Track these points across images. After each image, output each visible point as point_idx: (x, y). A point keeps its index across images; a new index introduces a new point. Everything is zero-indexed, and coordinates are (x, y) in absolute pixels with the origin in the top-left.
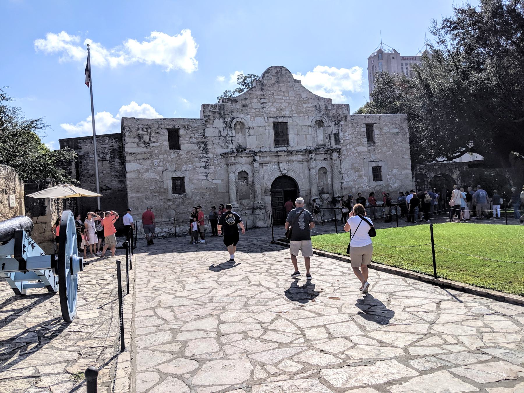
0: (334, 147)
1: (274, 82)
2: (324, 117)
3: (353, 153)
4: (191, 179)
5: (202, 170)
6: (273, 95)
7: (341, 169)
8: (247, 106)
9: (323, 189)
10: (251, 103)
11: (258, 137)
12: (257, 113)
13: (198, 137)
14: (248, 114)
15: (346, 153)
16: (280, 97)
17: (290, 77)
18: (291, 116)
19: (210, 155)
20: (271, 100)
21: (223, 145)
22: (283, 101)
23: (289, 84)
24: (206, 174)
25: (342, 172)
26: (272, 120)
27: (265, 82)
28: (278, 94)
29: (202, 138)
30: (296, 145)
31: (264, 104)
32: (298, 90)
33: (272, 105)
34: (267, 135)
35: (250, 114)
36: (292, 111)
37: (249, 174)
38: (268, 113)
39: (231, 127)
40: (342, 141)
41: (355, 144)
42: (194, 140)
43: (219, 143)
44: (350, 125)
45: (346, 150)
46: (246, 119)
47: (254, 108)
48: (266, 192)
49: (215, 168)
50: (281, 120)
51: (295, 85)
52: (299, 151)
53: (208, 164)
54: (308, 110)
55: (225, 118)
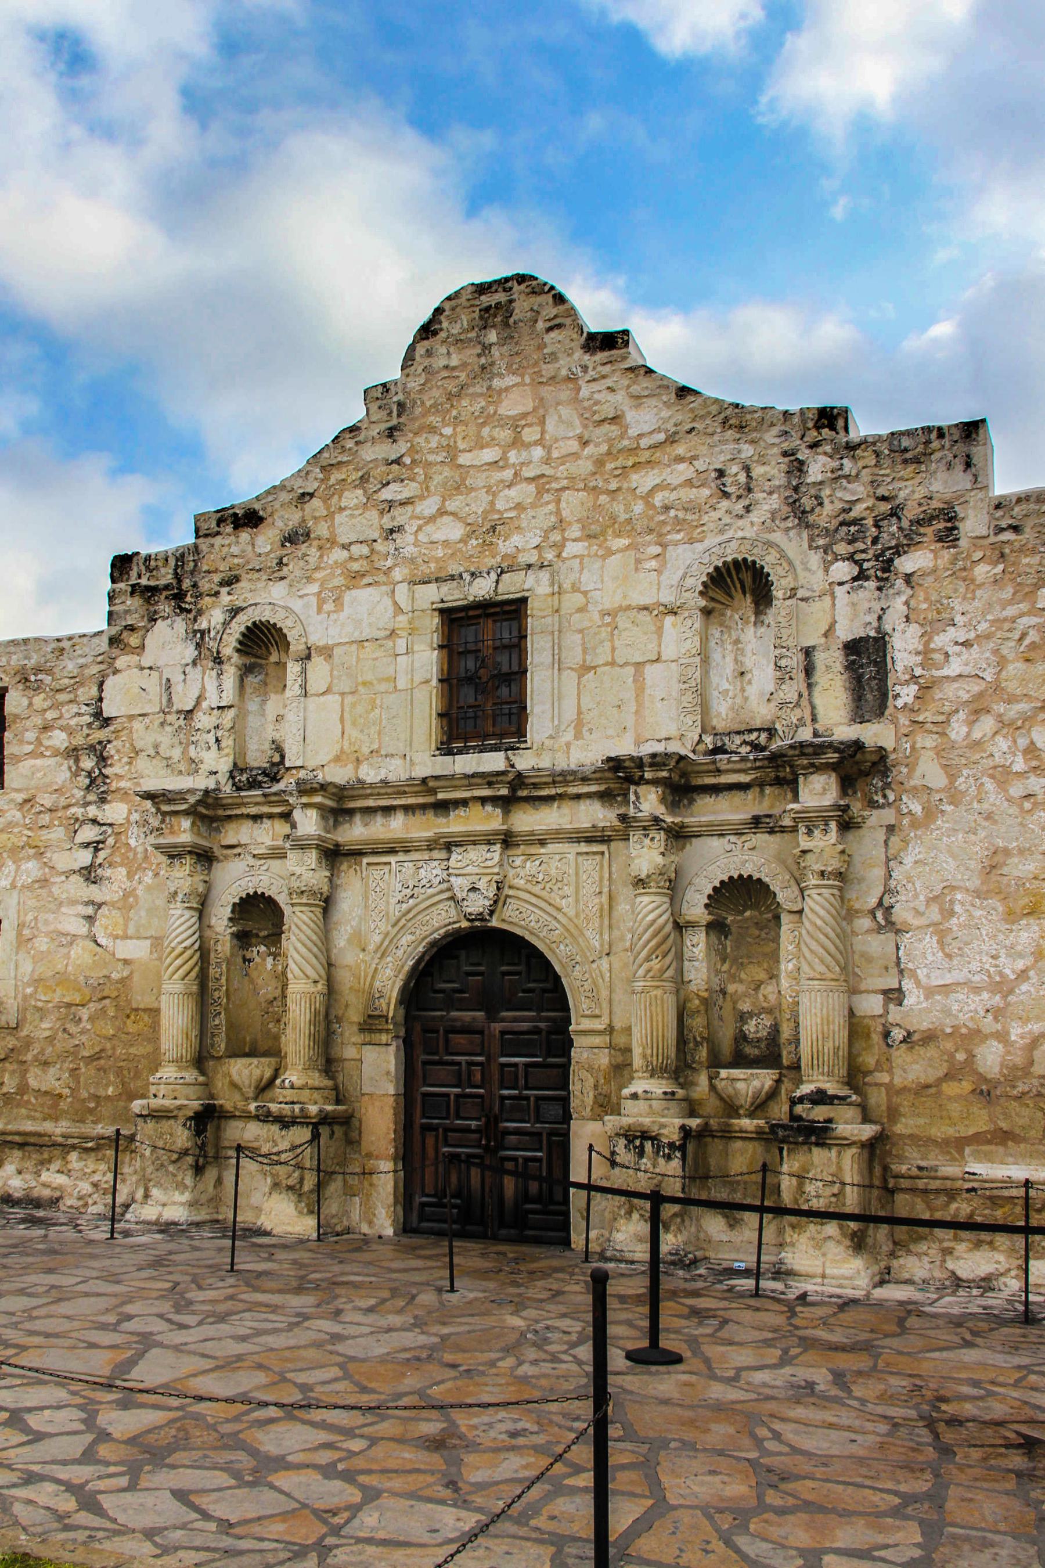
0: (845, 732)
1: (463, 376)
2: (777, 537)
3: (1003, 775)
4: (26, 932)
5: (77, 887)
6: (451, 451)
7: (887, 891)
8: (308, 535)
9: (776, 1029)
10: (330, 516)
11: (349, 699)
12: (355, 566)
13: (73, 722)
14: (309, 579)
15: (937, 778)
16: (489, 455)
17: (559, 326)
18: (549, 555)
19: (116, 811)
20: (437, 479)
21: (176, 753)
22: (508, 474)
23: (548, 370)
24: (90, 910)
25: (901, 914)
26: (431, 594)
27: (413, 384)
28: (479, 436)
29: (89, 725)
30: (569, 736)
31: (397, 512)
32: (610, 397)
33: (442, 512)
34: (401, 684)
35: (317, 575)
36: (561, 524)
37: (287, 910)
38: (412, 560)
39: (218, 660)
40: (907, 694)
41: (1023, 706)
42: (59, 739)
43: (156, 746)
44: (981, 571)
45: (939, 751)
46: (297, 605)
47: (343, 539)
48: (371, 1024)
49: (130, 876)
50: (482, 589)
51: (585, 368)
52: (564, 777)
53: (102, 855)
54: (667, 508)
55: (200, 612)
